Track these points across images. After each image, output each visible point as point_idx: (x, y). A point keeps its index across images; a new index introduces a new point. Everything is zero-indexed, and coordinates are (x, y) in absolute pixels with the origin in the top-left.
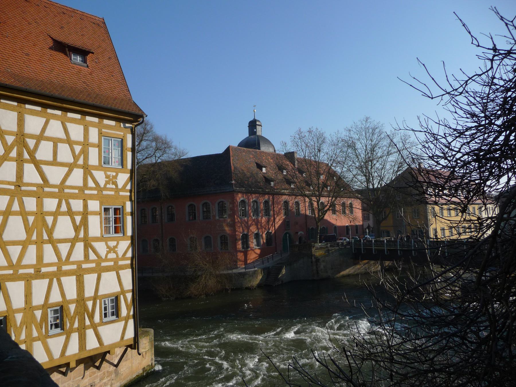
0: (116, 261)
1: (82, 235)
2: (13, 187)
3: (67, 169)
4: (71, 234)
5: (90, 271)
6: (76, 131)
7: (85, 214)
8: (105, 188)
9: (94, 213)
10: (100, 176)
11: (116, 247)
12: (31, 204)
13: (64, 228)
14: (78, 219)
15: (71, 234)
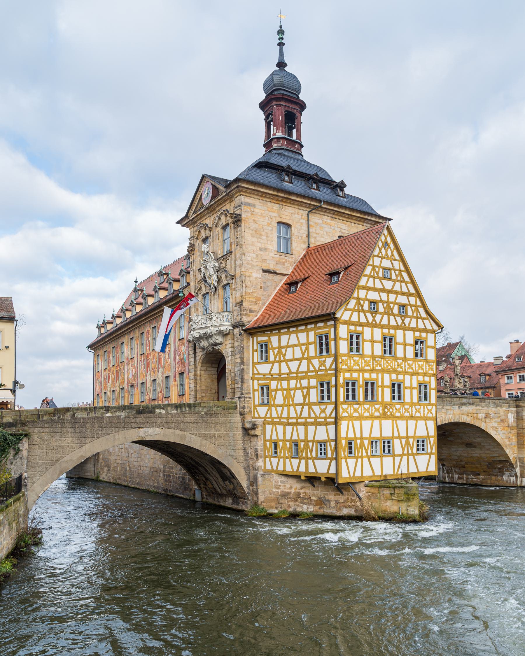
0: (325, 418)
1: (307, 401)
2: (278, 376)
3: (299, 361)
4: (302, 401)
5: (312, 424)
6: (303, 337)
7: (308, 388)
8: (319, 370)
9: (314, 387)
10: (316, 362)
11: (325, 409)
12: (284, 383)
13: (299, 397)
14: (305, 391)
15: (302, 401)
